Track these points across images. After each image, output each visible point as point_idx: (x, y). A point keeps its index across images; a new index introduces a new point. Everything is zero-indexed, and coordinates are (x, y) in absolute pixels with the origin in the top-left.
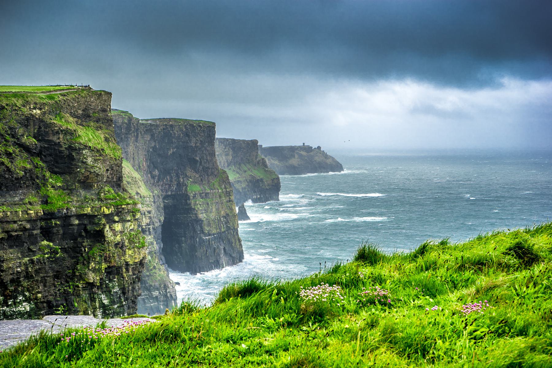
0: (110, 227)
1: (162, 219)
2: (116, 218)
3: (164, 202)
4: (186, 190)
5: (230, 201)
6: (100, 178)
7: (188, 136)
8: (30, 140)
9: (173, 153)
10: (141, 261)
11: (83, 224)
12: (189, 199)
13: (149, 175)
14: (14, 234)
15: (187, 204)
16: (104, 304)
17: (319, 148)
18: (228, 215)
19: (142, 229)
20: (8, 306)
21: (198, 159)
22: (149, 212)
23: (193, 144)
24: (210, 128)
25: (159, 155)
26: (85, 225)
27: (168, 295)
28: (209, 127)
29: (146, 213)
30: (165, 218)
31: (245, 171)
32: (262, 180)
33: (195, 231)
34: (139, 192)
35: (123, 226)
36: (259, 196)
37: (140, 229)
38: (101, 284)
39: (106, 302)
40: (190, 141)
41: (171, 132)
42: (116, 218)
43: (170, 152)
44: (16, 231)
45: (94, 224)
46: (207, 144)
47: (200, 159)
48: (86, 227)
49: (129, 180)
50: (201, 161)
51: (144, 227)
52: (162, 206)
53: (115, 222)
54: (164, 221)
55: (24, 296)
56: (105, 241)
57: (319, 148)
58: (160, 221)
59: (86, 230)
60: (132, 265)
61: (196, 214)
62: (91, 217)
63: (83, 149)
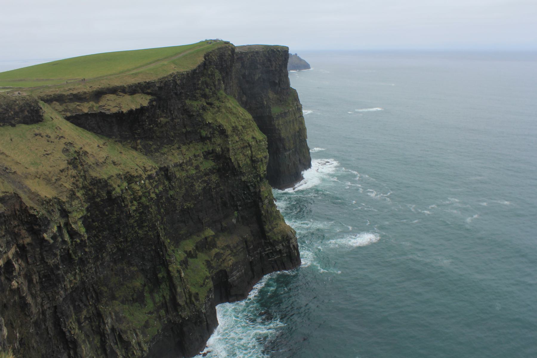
7: (270, 61)
9: (259, 78)
12: (274, 120)
17: (296, 54)
21: (277, 81)
27: (292, 246)
29: (263, 159)
34: (255, 136)
37: (259, 179)
40: (272, 65)
41: (257, 58)
43: (257, 78)
49: (244, 124)
50: (279, 84)
57: (296, 54)
61: (280, 134)
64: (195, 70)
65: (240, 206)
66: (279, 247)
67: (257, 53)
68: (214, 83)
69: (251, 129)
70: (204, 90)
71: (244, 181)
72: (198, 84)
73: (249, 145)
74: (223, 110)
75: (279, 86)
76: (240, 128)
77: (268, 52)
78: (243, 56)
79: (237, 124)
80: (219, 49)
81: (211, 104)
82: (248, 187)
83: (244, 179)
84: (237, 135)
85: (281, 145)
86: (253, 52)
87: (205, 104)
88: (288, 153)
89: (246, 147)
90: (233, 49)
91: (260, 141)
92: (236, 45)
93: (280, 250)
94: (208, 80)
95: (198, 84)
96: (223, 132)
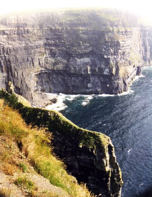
39: (105, 47)
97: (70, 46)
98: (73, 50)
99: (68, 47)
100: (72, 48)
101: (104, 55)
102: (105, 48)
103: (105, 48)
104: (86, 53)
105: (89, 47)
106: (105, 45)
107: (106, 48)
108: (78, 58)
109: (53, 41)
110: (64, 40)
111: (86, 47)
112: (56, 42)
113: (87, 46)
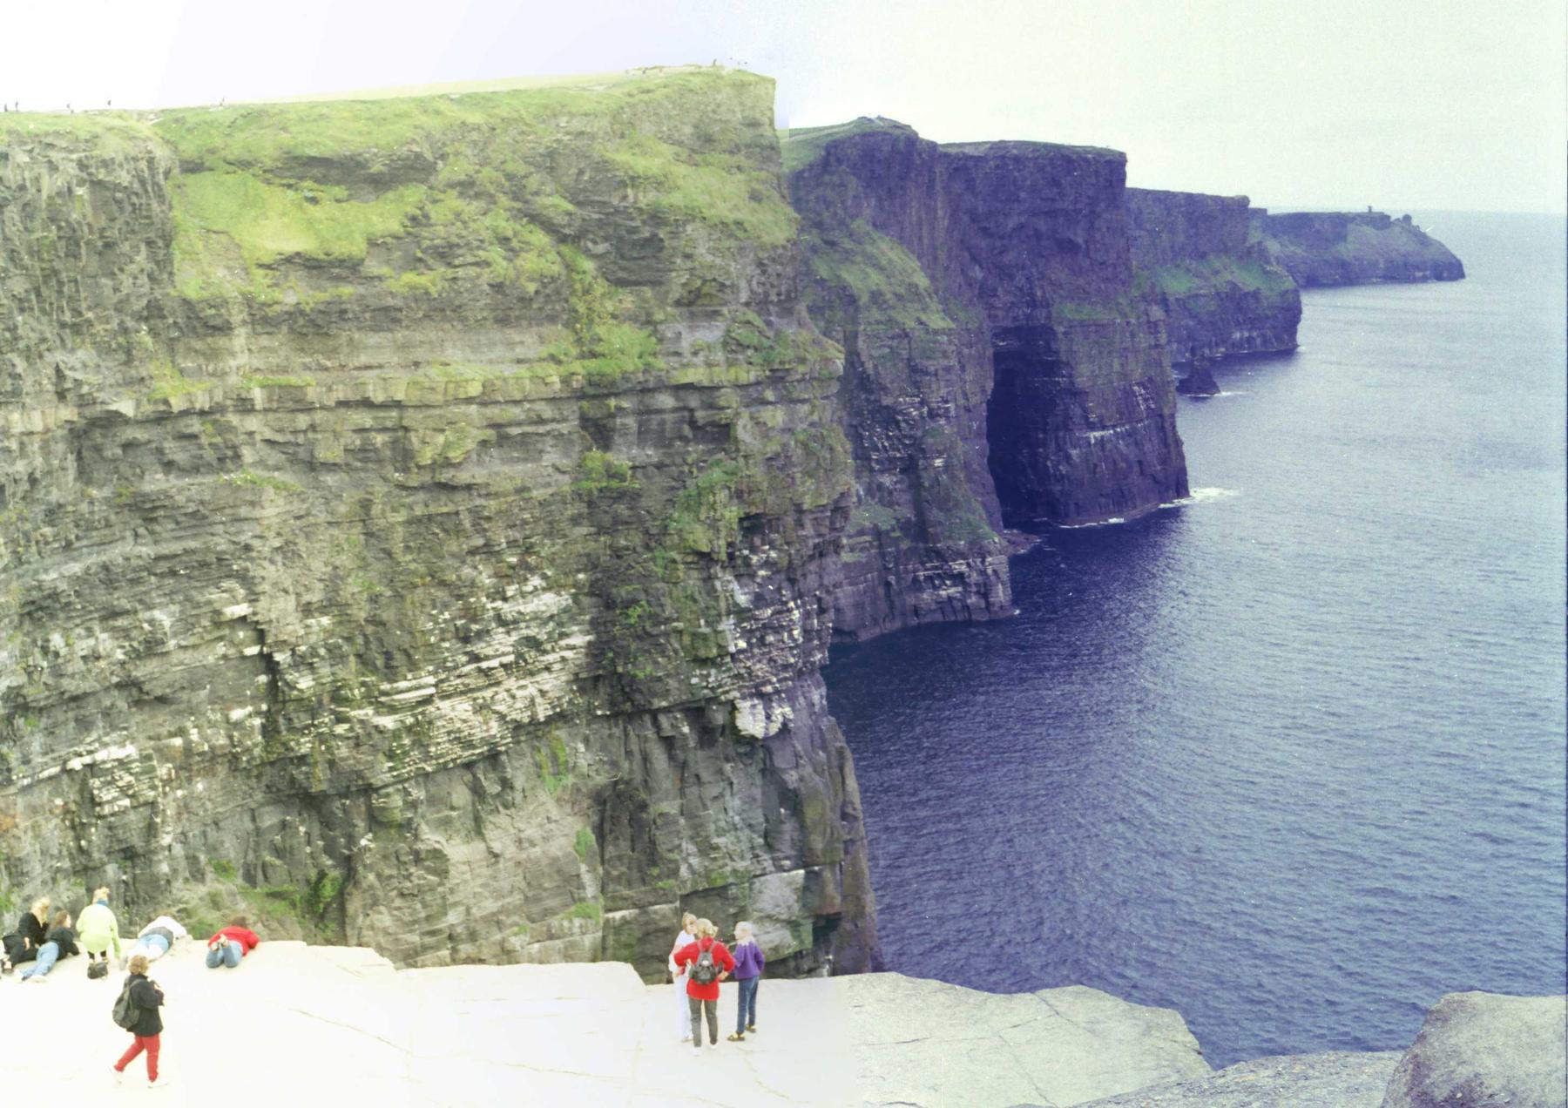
0: (752, 418)
1: (990, 385)
2: (770, 395)
3: (995, 345)
4: (1049, 317)
5: (1156, 346)
6: (728, 296)
7: (1056, 183)
8: (555, 204)
9: (1022, 226)
10: (836, 501)
11: (685, 408)
13: (960, 279)
14: (514, 431)
15: (1049, 351)
16: (736, 604)
17: (1407, 218)
18: (1150, 380)
19: (930, 411)
20: (505, 599)
21: (1080, 240)
22: (948, 369)
23: (1066, 204)
24: (1114, 165)
25: (986, 232)
26: (691, 411)
27: (990, 571)
28: (1109, 162)
30: (996, 384)
31: (1216, 272)
32: (1255, 295)
33: (1068, 418)
35: (791, 415)
36: (1246, 334)
37: (925, 410)
38: (731, 557)
39: (743, 599)
42: (770, 395)
43: (1012, 223)
44: (519, 424)
45: (712, 406)
46: (1103, 205)
47: (1086, 242)
48: (692, 416)
49: (902, 291)
51: (934, 405)
52: (990, 352)
53: (766, 403)
54: (994, 391)
55: (544, 577)
56: (738, 450)
57: (1407, 218)
58: (983, 391)
59: (692, 423)
60: (811, 512)
61: (1070, 376)
62: (707, 391)
63: (685, 222)
64: (802, 172)
65: (878, 461)
66: (959, 566)
67: (1016, 159)
68: (843, 202)
69: (917, 306)
70: (819, 215)
71: (887, 407)
72: (808, 201)
73: (907, 335)
74: (858, 258)
75: (1087, 255)
76: (889, 296)
77: (1051, 160)
78: (971, 164)
79: (884, 288)
80: (864, 135)
81: (832, 244)
82: (897, 423)
83: (887, 401)
84: (880, 308)
85: (1078, 411)
86: (1003, 157)
87: (818, 241)
88: (1098, 434)
89: (899, 336)
90: (911, 140)
91: (936, 332)
92: (922, 135)
93: (961, 575)
94: (830, 194)
95: (808, 201)
96: (852, 300)
97: (336, 655)
98: (388, 722)
99: (305, 683)
100: (372, 698)
101: (732, 708)
102: (741, 614)
103: (741, 614)
104: (533, 721)
105: (560, 620)
106: (745, 574)
107: (759, 600)
108: (445, 823)
109: (105, 641)
110: (253, 598)
111: (533, 643)
112: (152, 647)
113: (540, 619)
